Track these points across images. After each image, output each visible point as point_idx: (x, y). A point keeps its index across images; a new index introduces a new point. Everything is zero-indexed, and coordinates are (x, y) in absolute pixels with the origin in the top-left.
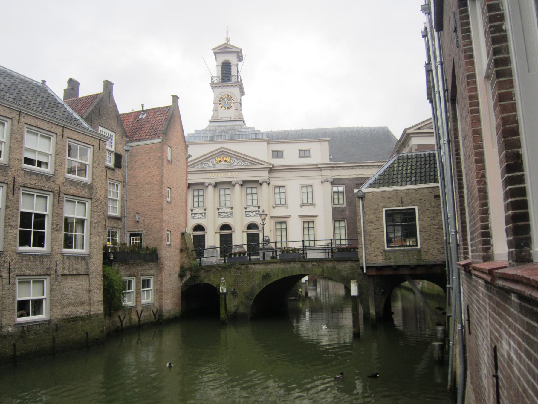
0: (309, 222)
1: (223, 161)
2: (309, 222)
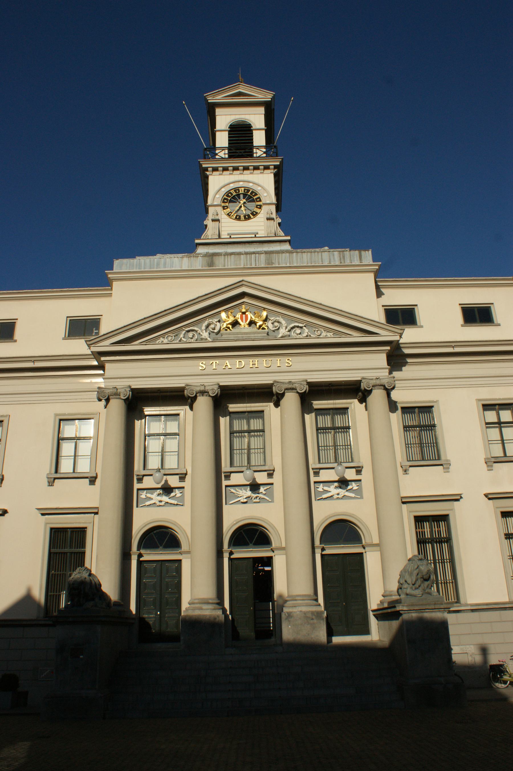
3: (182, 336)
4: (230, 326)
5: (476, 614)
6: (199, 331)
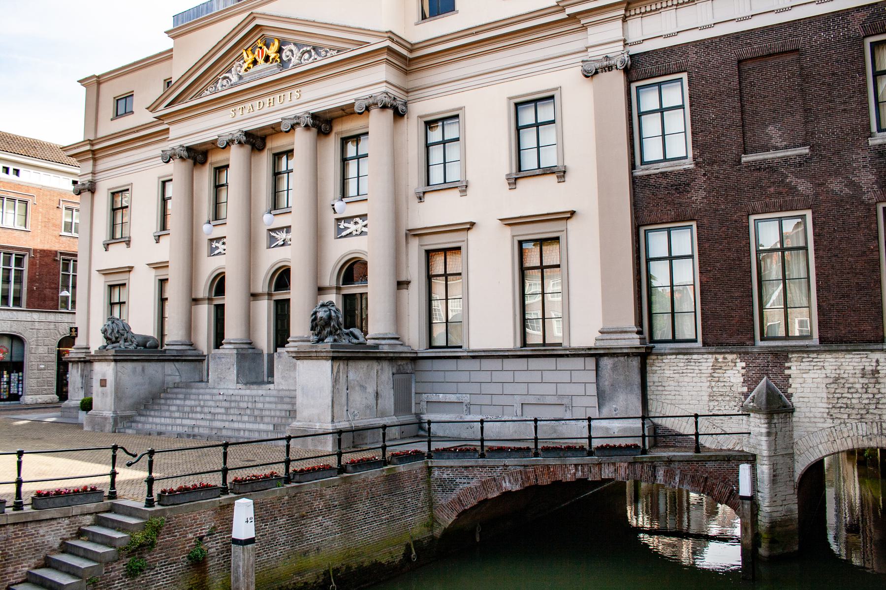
0: (536, 246)
1: (261, 61)
2: (536, 246)
3: (219, 85)
4: (251, 66)
5: (478, 361)
6: (231, 77)
